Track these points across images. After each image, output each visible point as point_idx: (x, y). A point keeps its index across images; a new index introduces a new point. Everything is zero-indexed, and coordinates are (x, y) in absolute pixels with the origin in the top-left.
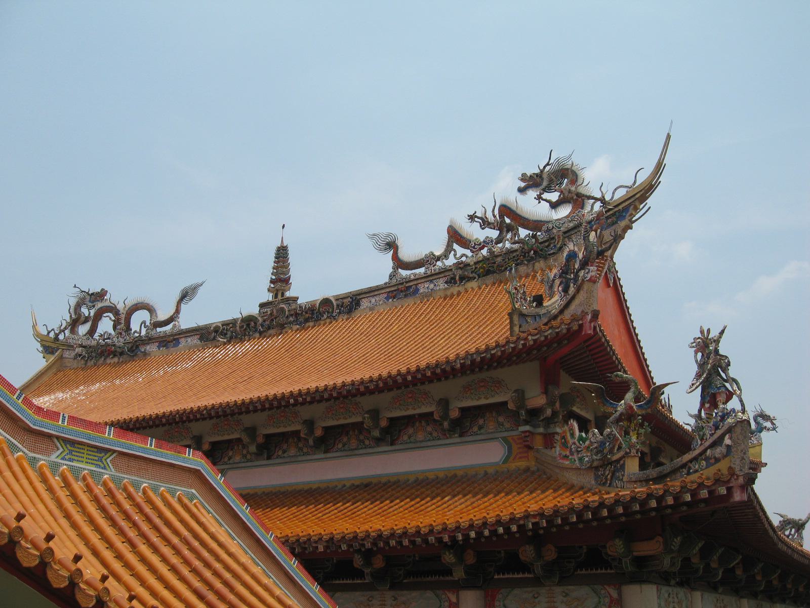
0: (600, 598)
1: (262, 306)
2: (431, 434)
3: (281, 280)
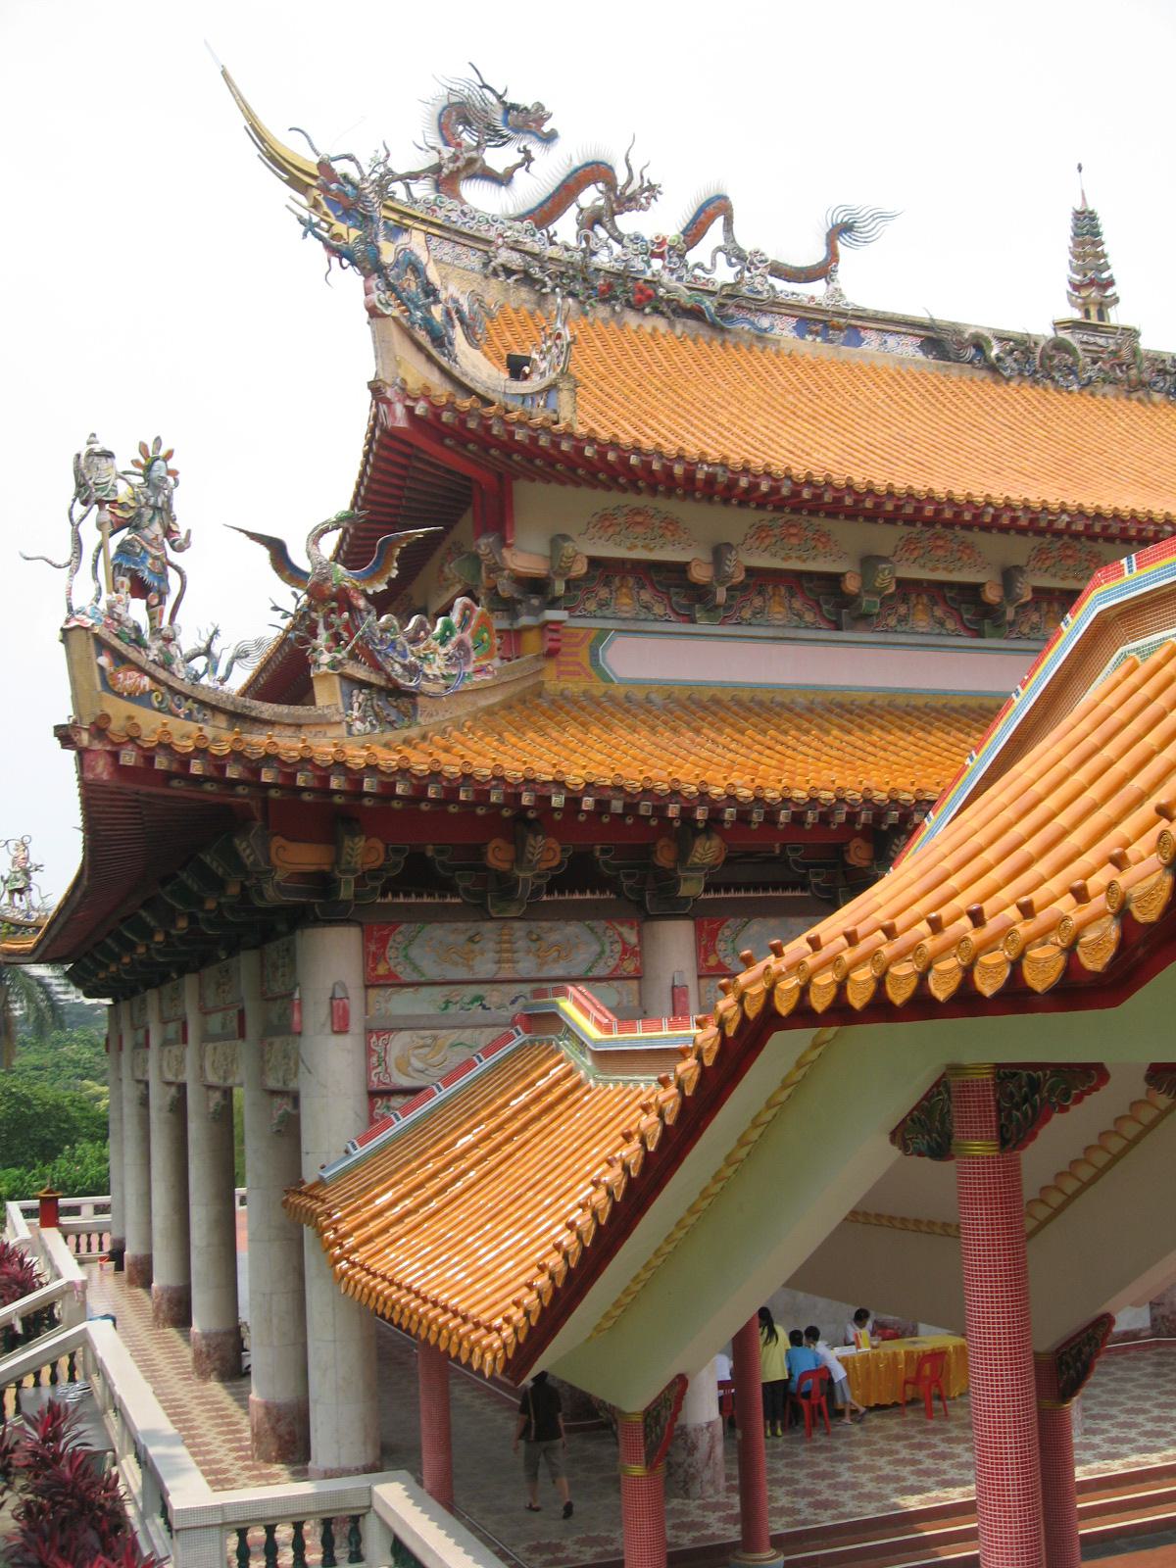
0: (602, 945)
1: (1074, 326)
2: (800, 617)
3: (1092, 280)
